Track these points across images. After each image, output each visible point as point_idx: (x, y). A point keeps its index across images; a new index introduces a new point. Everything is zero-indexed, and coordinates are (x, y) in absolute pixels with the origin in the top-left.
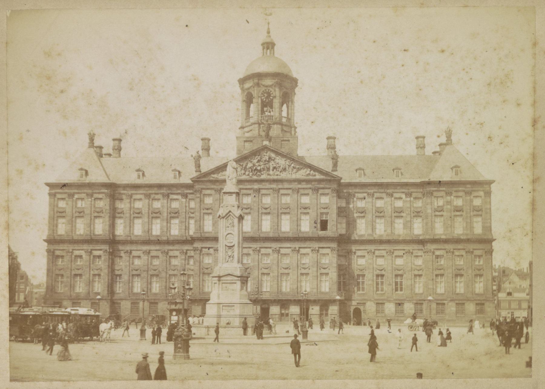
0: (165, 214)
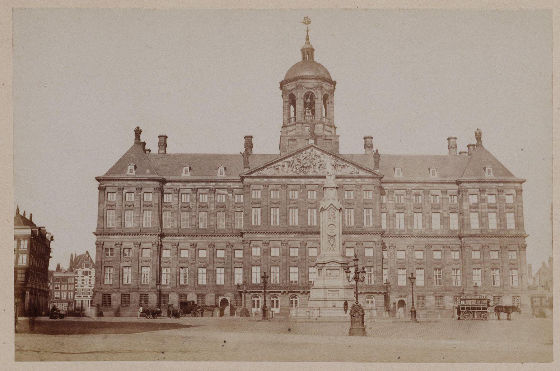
0: (212, 209)
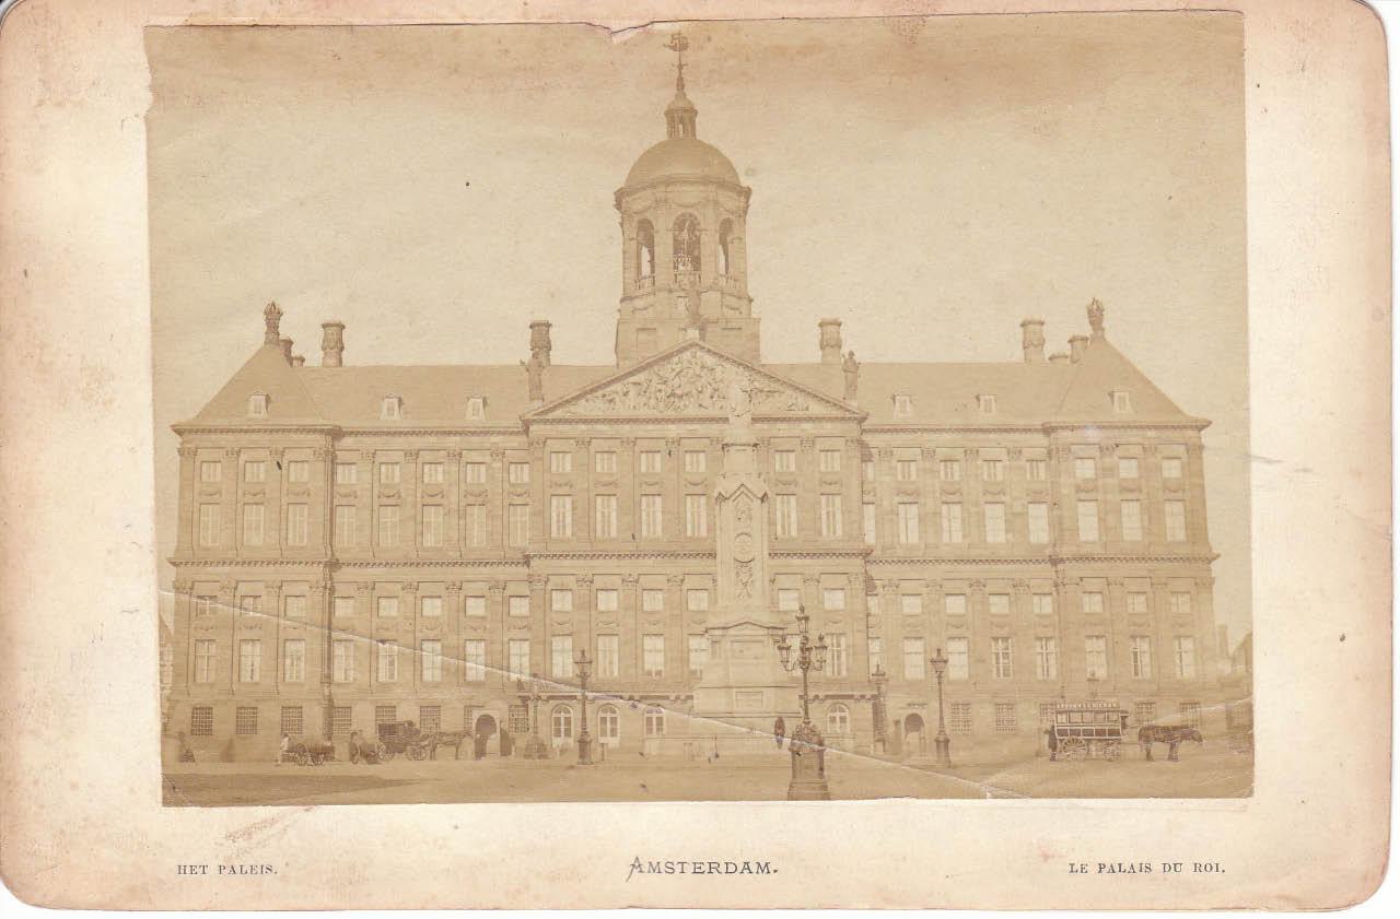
0: (454, 499)
